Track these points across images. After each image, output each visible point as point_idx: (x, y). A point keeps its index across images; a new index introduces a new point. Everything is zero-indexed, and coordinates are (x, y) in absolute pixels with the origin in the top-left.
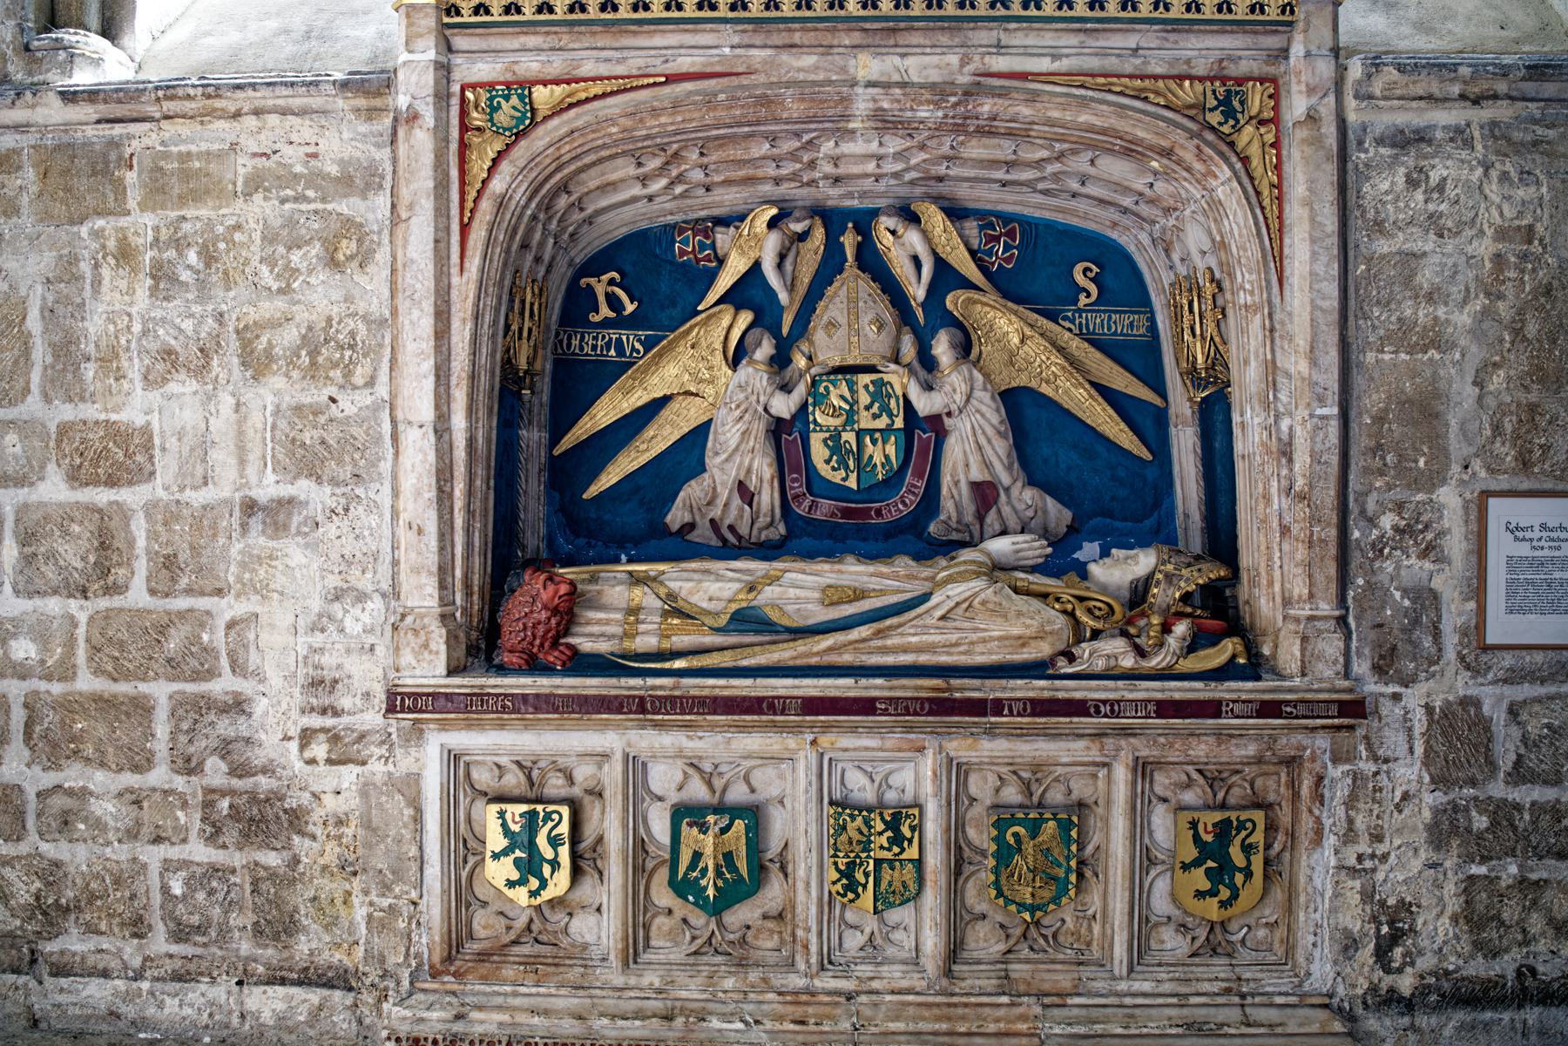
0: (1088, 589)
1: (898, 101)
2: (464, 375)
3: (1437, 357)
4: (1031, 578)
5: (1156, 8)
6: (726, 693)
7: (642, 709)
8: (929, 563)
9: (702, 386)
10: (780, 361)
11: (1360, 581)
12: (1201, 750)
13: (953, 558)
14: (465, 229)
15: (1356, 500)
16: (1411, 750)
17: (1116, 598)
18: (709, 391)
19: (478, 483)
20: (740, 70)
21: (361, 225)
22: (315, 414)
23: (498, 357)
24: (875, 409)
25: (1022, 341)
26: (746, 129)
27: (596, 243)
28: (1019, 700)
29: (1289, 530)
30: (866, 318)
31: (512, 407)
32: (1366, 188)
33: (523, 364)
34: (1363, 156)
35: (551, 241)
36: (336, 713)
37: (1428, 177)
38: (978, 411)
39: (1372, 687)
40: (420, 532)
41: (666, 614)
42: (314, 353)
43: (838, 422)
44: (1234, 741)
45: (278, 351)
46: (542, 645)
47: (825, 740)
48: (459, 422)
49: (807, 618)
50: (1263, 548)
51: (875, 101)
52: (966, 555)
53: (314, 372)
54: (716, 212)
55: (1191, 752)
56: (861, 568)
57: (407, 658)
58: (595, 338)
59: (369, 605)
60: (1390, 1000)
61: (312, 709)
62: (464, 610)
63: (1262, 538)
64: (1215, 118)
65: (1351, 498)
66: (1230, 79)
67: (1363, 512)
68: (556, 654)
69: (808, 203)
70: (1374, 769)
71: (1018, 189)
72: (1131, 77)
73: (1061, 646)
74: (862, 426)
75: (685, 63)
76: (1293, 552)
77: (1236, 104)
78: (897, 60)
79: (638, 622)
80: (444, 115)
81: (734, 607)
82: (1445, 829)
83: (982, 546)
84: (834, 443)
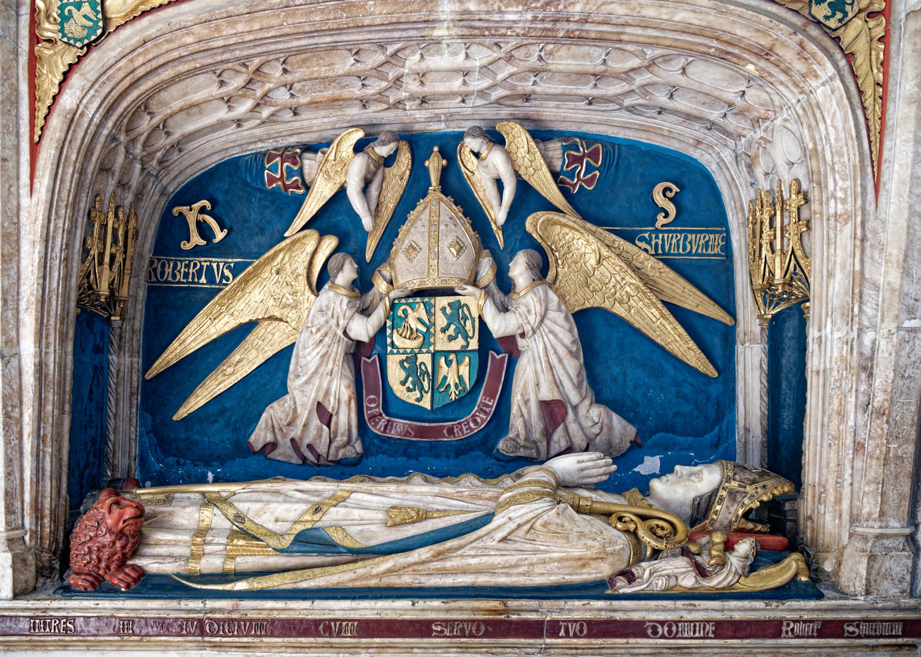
0: (650, 506)
4: (594, 495)
8: (494, 481)
9: (285, 311)
13: (519, 476)
17: (678, 515)
18: (292, 315)
24: (451, 331)
25: (599, 262)
27: (189, 172)
28: (576, 621)
29: (863, 446)
30: (446, 241)
31: (103, 334)
35: (138, 166)
38: (551, 332)
41: (233, 535)
43: (415, 344)
46: (108, 567)
52: (533, 473)
54: (306, 138)
56: (426, 488)
58: (187, 266)
62: (34, 533)
63: (833, 455)
69: (395, 128)
71: (604, 107)
74: (439, 347)
76: (865, 471)
79: (205, 543)
81: (299, 528)
83: (548, 464)
84: (411, 364)
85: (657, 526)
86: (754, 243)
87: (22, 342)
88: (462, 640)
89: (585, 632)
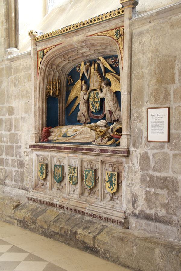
14: (38, 74)
16: (137, 162)
19: (41, 113)
60: (135, 215)
64: (115, 37)
72: (104, 32)
75: (57, 43)
82: (143, 179)
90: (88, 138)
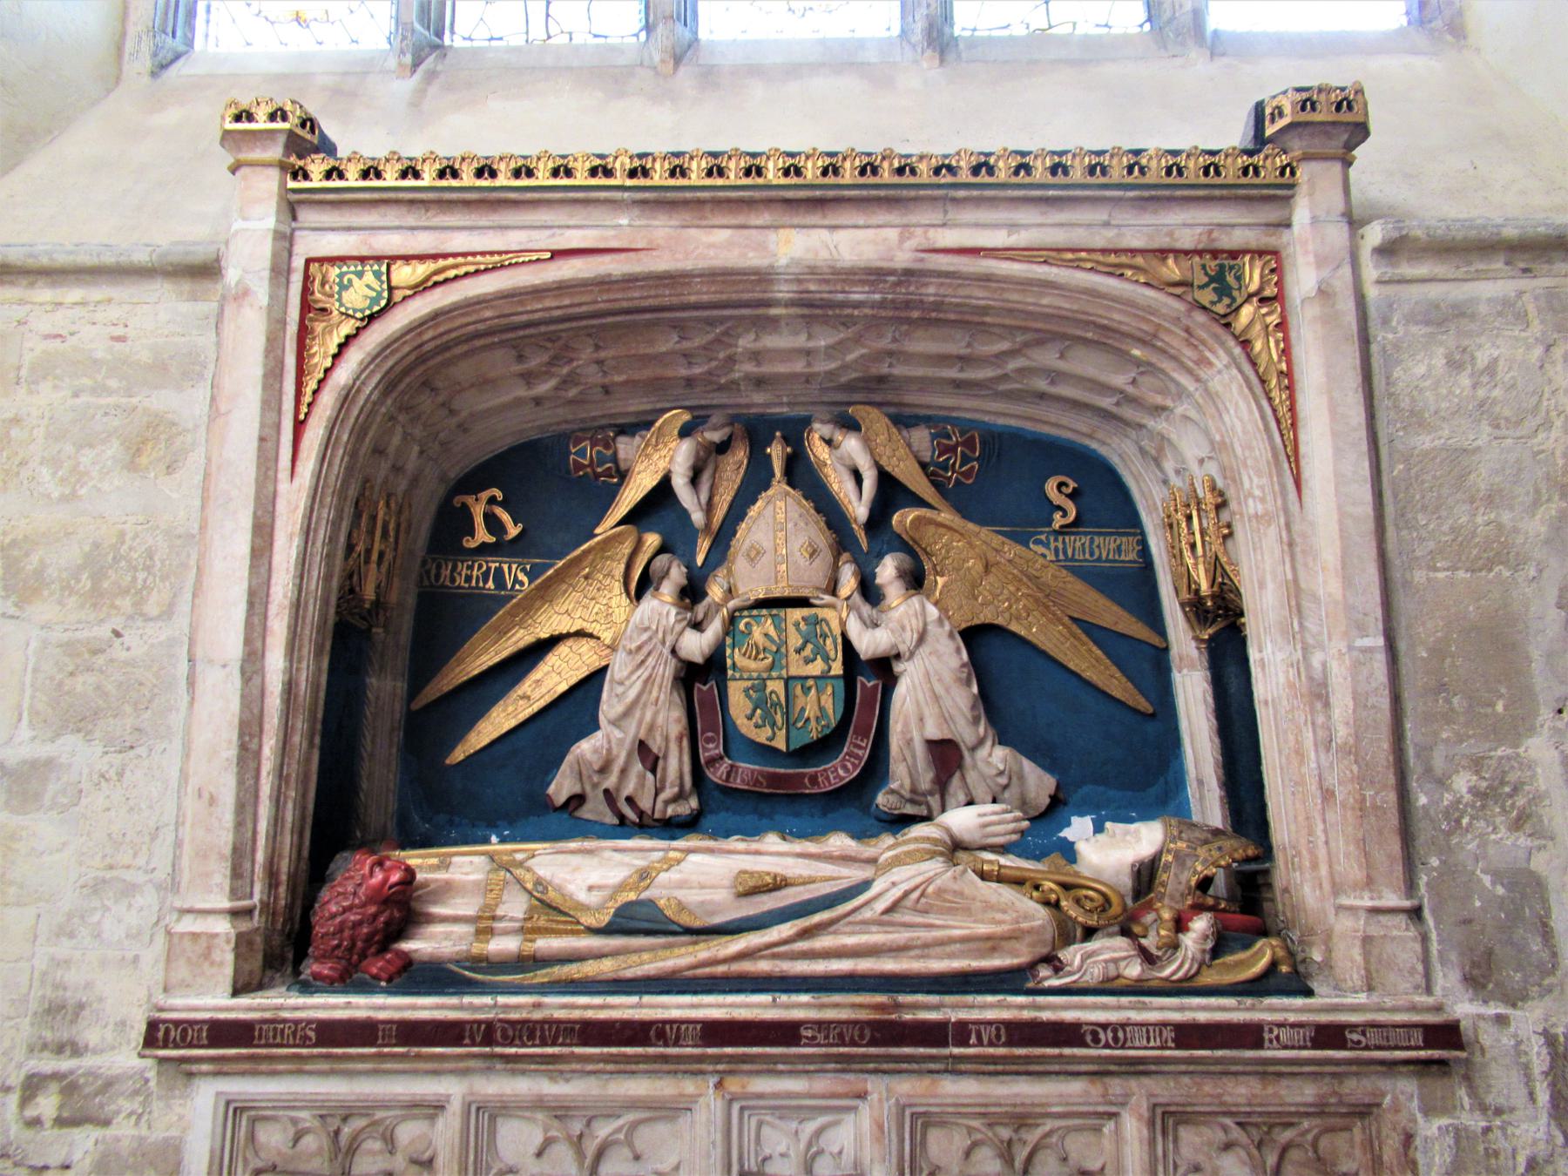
1: (826, 281)
2: (287, 603)
3: (1506, 573)
5: (1130, 172)
6: (602, 1015)
7: (488, 1040)
10: (692, 593)
11: (1435, 862)
12: (1240, 1092)
14: (299, 426)
15: (1418, 756)
16: (1532, 1096)
19: (297, 739)
20: (639, 246)
21: (174, 424)
22: (95, 652)
23: (335, 583)
26: (648, 316)
28: (989, 1023)
29: (1333, 793)
32: (1397, 373)
33: (369, 593)
34: (1390, 336)
36: (76, 1050)
37: (1473, 358)
39: (1464, 1009)
40: (213, 801)
42: (97, 577)
44: (1285, 1082)
45: (52, 572)
47: (733, 1085)
48: (275, 661)
49: (713, 913)
50: (1301, 818)
51: (800, 281)
53: (96, 597)
55: (1227, 1099)
56: (784, 847)
57: (182, 972)
59: (139, 900)
61: (45, 1046)
64: (1207, 297)
65: (1411, 752)
66: (1223, 251)
67: (1428, 770)
68: (380, 964)
70: (1484, 1124)
73: (1044, 950)
75: (574, 239)
77: (1230, 279)
78: (824, 234)
80: (282, 292)
85: (1086, 897)
86: (1173, 547)
87: (268, 654)
88: (842, 1050)
89: (1003, 1039)
90: (990, 944)
